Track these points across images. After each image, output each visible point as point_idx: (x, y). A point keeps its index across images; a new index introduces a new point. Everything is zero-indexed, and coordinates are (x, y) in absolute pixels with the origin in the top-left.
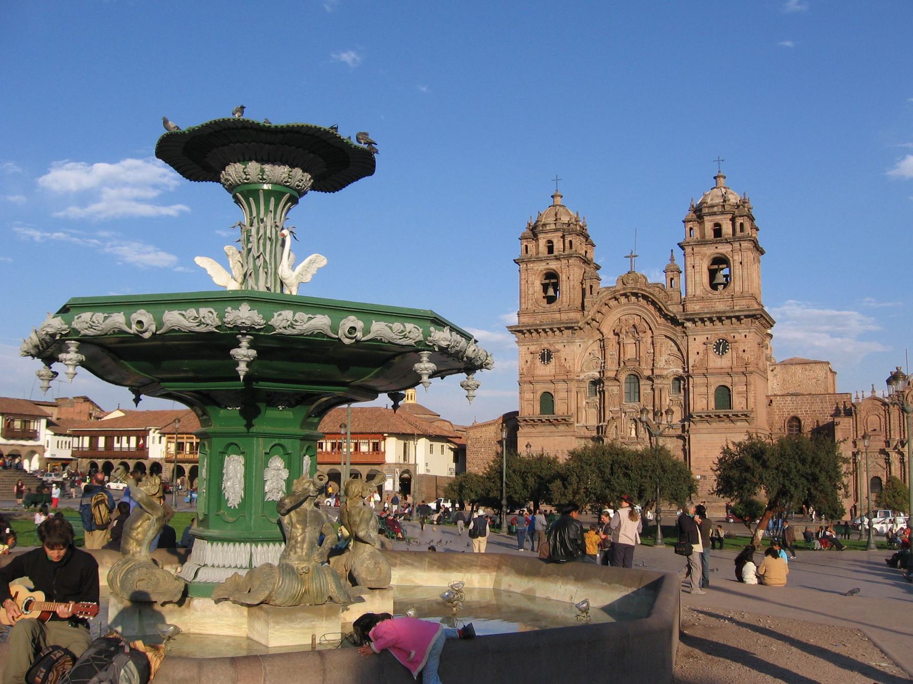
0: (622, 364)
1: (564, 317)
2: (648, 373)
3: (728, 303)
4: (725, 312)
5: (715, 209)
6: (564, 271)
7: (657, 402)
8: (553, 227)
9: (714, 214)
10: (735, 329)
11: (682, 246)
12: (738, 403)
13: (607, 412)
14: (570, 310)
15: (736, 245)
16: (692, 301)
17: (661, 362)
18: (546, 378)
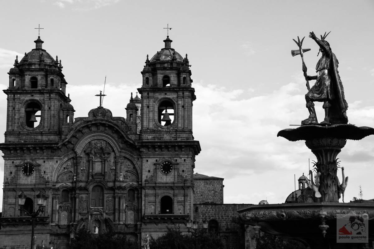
0: (90, 178)
1: (45, 138)
2: (110, 185)
3: (173, 135)
4: (171, 142)
5: (166, 65)
6: (46, 103)
7: (117, 207)
8: (37, 66)
9: (165, 69)
10: (178, 155)
12: (178, 210)
13: (77, 214)
15: (181, 94)
16: (146, 132)
18: (28, 187)
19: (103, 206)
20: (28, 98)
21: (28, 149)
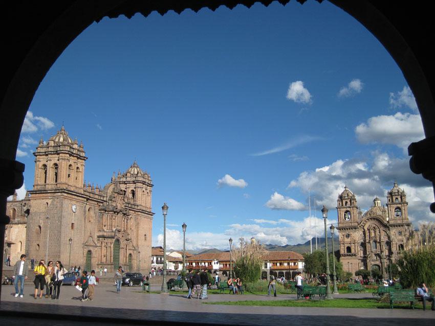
1: (353, 224)
9: (396, 195)
11: (387, 205)
17: (382, 238)
20: (345, 209)
21: (347, 229)
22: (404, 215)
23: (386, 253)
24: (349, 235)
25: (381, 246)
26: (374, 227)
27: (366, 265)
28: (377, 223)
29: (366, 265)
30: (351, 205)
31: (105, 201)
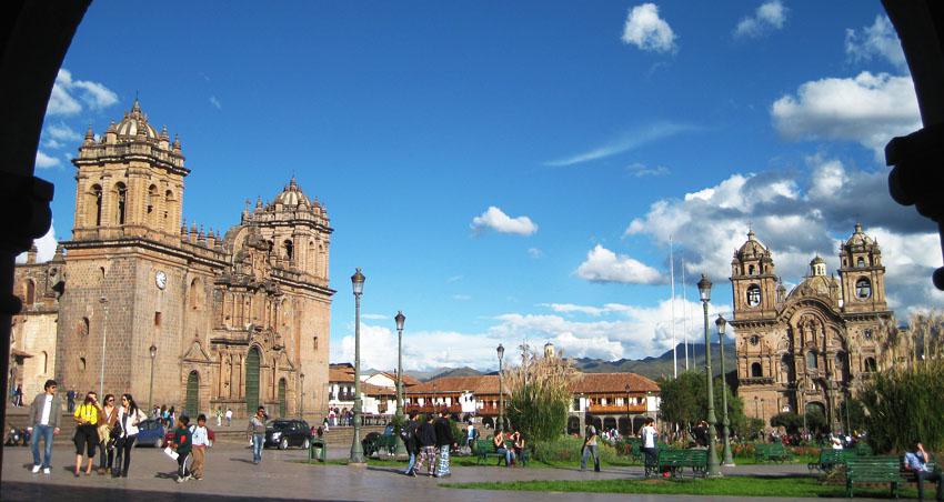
9: (859, 252)
11: (840, 273)
14: (769, 311)
19: (816, 366)
20: (749, 282)
21: (753, 325)
22: (876, 294)
23: (838, 376)
24: (757, 337)
25: (826, 361)
26: (812, 321)
27: (793, 403)
28: (818, 312)
29: (793, 403)
30: (761, 271)
31: (227, 264)
